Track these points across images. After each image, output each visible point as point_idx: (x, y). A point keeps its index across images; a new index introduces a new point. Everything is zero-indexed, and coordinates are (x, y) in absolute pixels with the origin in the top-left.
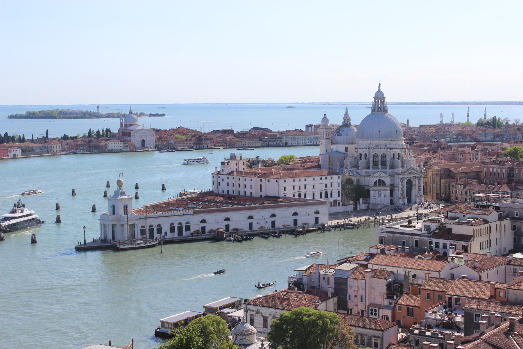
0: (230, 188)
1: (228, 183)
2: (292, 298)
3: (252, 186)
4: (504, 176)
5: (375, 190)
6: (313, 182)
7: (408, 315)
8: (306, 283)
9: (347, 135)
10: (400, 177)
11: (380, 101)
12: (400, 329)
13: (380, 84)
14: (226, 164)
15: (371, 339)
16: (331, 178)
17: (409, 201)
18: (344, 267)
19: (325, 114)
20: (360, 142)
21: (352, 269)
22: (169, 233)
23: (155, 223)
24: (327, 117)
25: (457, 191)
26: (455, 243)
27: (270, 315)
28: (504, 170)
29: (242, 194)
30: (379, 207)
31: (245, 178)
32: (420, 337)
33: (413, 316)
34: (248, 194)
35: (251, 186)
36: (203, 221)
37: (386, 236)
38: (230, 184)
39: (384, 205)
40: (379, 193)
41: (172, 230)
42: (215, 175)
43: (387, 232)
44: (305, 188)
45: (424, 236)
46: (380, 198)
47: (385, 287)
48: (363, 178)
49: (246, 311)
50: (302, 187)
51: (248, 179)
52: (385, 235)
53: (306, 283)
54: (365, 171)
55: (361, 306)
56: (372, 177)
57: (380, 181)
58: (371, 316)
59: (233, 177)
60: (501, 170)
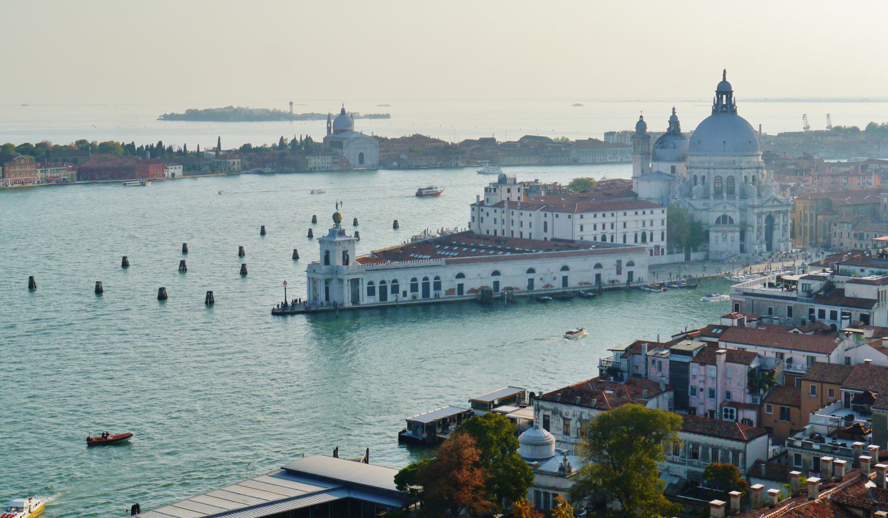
0: (498, 227)
1: (495, 219)
2: (607, 392)
3: (533, 225)
5: (718, 231)
6: (625, 219)
7: (782, 417)
8: (626, 370)
9: (674, 147)
10: (756, 211)
11: (724, 96)
12: (770, 442)
13: (725, 71)
14: (493, 190)
15: (728, 453)
16: (652, 213)
17: (769, 248)
18: (683, 345)
19: (641, 117)
20: (694, 159)
21: (697, 349)
22: (409, 294)
23: (389, 277)
25: (842, 233)
26: (849, 312)
27: (574, 416)
29: (517, 235)
30: (724, 257)
31: (521, 211)
32: (804, 451)
33: (788, 419)
34: (526, 236)
35: (530, 223)
36: (460, 276)
37: (744, 300)
38: (499, 221)
40: (723, 235)
41: (414, 288)
42: (474, 207)
43: (746, 294)
44: (612, 227)
45: (802, 301)
46: (724, 243)
47: (747, 377)
49: (538, 410)
50: (608, 226)
51: (526, 213)
52: (742, 299)
53: (626, 370)
54: (702, 202)
55: (710, 405)
56: (713, 211)
57: (725, 217)
58: (724, 419)
59: (503, 209)
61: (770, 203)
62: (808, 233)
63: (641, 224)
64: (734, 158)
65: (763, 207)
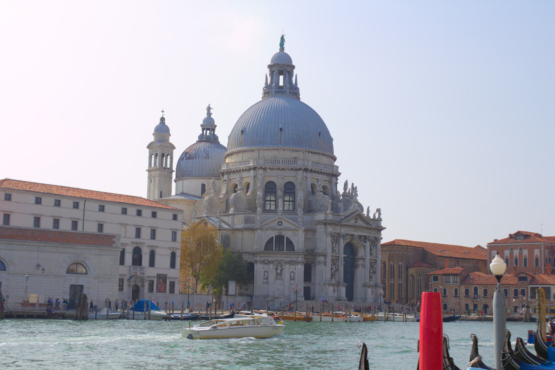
4: (537, 265)
5: (269, 262)
10: (330, 229)
13: (283, 39)
16: (154, 215)
17: (350, 296)
19: (163, 119)
24: (167, 123)
25: (445, 290)
28: (537, 252)
39: (289, 299)
40: (277, 269)
46: (278, 281)
48: (239, 235)
56: (261, 229)
57: (280, 238)
60: (531, 252)
61: (352, 222)
62: (396, 293)
63: (132, 232)
64: (295, 154)
65: (341, 225)
